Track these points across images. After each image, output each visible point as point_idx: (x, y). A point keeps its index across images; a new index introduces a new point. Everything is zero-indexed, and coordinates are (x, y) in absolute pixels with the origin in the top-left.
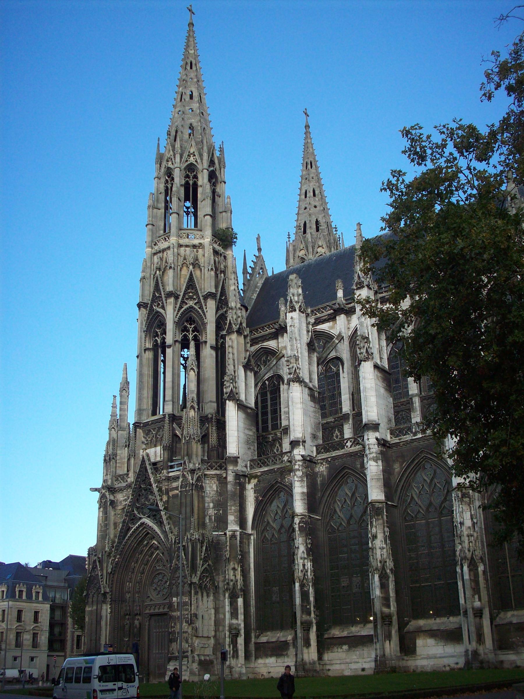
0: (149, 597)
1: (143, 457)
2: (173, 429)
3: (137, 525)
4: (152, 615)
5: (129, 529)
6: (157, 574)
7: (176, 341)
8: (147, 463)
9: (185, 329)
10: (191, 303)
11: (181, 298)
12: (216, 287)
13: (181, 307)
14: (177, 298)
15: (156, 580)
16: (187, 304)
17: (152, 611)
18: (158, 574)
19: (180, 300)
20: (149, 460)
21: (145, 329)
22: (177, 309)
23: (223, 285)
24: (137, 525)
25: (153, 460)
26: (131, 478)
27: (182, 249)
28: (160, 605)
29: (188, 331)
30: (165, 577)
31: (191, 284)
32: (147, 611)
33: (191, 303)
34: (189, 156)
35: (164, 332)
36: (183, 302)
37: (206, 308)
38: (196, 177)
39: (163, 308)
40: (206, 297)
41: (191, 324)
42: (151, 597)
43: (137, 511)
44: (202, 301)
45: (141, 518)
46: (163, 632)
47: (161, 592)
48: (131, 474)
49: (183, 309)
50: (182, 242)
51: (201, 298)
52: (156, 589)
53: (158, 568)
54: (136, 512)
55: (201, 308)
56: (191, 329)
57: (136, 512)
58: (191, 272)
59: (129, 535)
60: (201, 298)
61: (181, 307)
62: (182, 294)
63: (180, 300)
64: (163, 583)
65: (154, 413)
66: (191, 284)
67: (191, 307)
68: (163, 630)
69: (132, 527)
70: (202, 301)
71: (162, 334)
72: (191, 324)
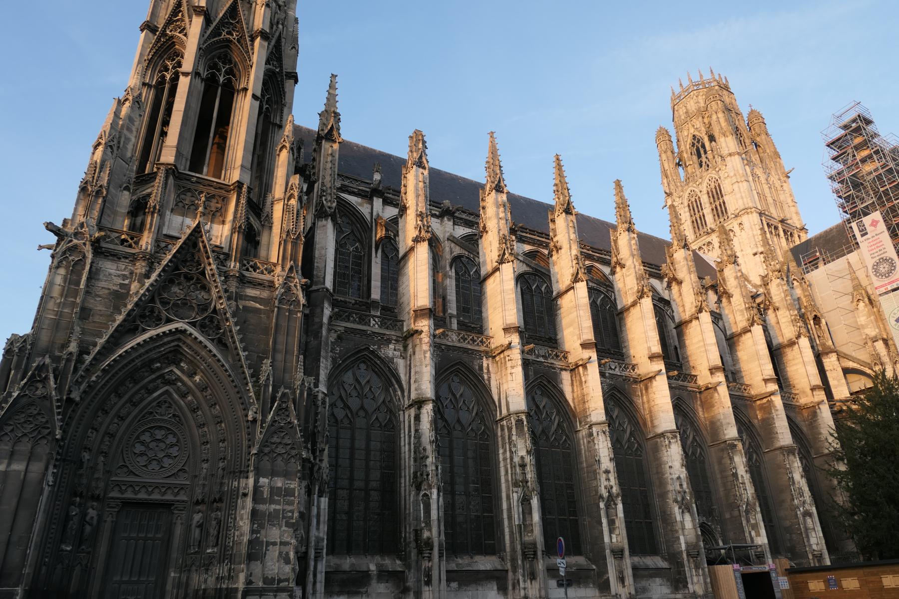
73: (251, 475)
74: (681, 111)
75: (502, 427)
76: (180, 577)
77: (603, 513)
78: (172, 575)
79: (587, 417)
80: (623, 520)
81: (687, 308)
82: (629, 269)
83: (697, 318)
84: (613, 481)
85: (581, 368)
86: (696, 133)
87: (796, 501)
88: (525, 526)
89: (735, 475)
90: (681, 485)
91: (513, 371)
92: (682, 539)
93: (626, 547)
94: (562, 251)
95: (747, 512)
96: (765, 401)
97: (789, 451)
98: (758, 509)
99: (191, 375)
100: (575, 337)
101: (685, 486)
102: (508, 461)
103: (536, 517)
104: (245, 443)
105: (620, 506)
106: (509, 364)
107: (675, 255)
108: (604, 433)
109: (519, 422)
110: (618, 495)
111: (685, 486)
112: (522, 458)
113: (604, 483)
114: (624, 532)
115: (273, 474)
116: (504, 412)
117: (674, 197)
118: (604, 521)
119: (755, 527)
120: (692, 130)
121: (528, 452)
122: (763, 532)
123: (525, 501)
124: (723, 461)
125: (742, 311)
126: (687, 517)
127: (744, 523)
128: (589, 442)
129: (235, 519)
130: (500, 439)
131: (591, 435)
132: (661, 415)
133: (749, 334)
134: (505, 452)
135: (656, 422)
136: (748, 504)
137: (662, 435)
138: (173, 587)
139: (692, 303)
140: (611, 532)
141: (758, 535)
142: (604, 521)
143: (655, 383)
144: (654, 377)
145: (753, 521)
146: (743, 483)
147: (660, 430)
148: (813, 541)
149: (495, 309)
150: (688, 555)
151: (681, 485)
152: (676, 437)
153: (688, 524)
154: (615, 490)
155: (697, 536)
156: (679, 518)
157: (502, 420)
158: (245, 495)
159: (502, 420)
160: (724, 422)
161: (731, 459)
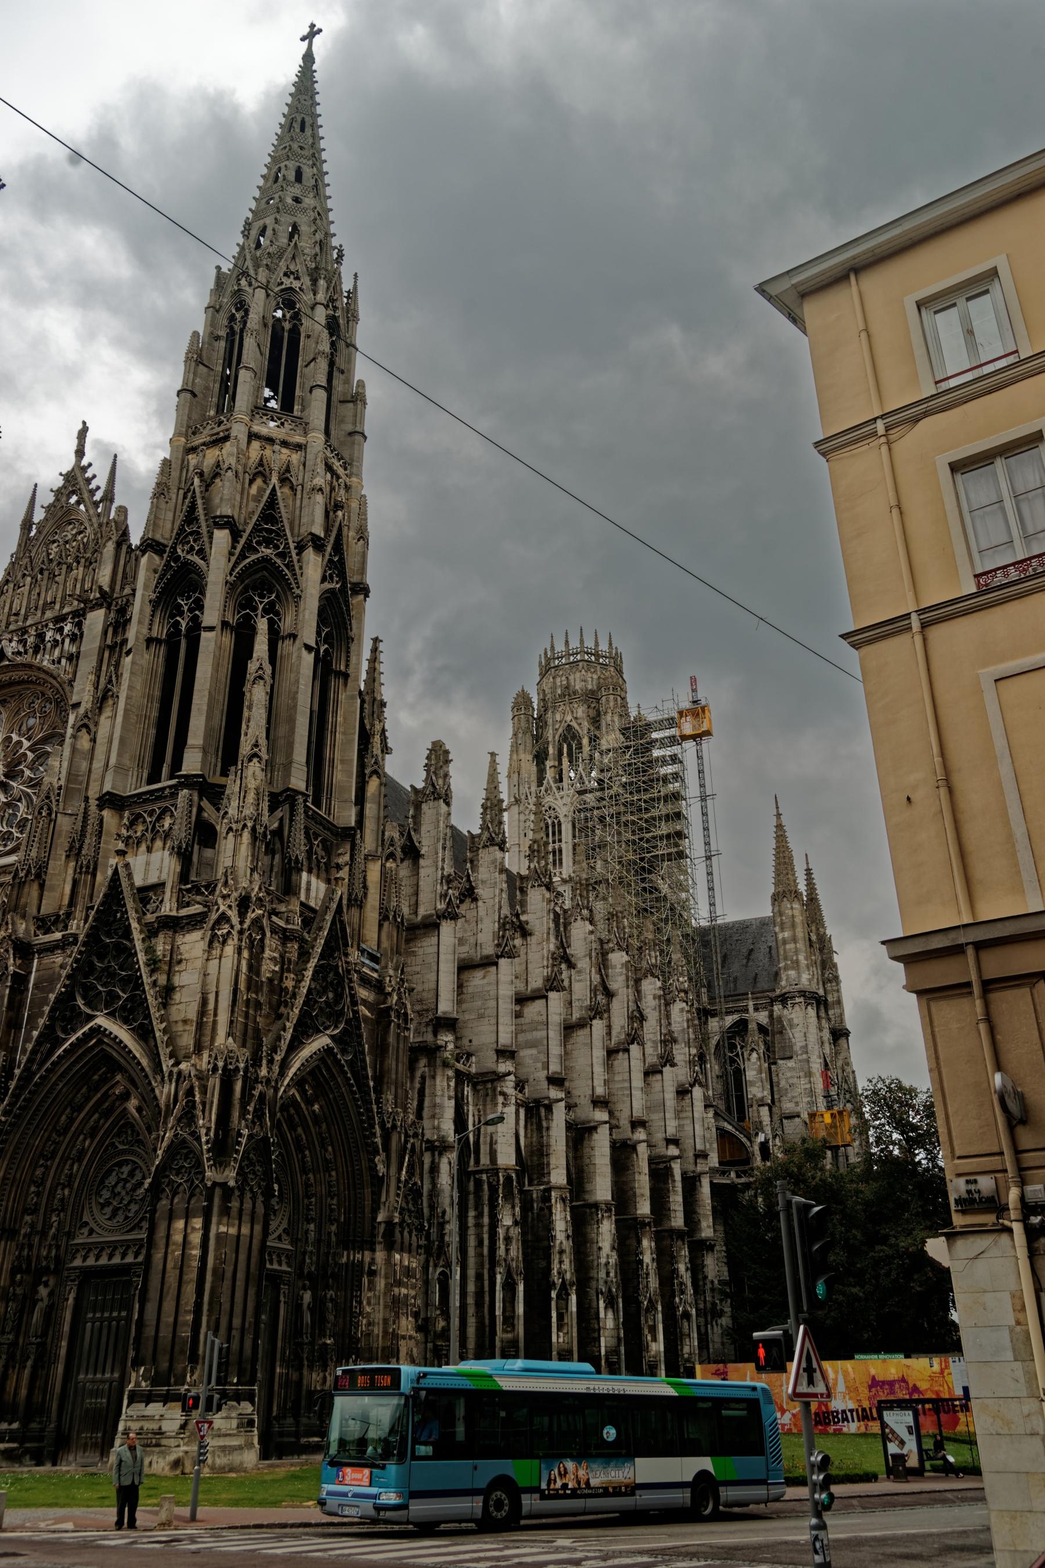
0: (87, 1224)
1: (116, 872)
2: (200, 810)
3: (79, 1034)
4: (87, 1275)
5: (58, 1042)
6: (116, 1165)
7: (225, 624)
8: (124, 883)
9: (248, 604)
10: (266, 551)
11: (245, 536)
12: (327, 530)
13: (242, 556)
14: (236, 535)
15: (112, 1180)
16: (257, 551)
17: (91, 1261)
18: (120, 1164)
19: (242, 541)
20: (130, 876)
21: (153, 596)
22: (233, 559)
23: (340, 529)
24: (79, 1034)
25: (138, 882)
26: (78, 926)
27: (256, 444)
28: (114, 1246)
29: (255, 609)
30: (137, 1172)
31: (270, 511)
32: (78, 1262)
33: (266, 551)
34: (286, 274)
35: (199, 605)
36: (249, 548)
37: (301, 568)
38: (296, 316)
39: (202, 553)
40: (301, 548)
41: (262, 596)
42: (92, 1225)
43: (84, 998)
44: (294, 553)
45: (91, 1018)
46: (114, 1319)
47: (120, 1212)
48: (79, 913)
49: (248, 561)
50: (256, 428)
51: (292, 546)
52: (108, 1203)
53: (121, 1147)
54: (80, 1002)
55: (290, 566)
56: (261, 607)
57: (80, 1002)
58: (274, 489)
59: (54, 1058)
60: (292, 546)
61: (242, 556)
62: (248, 532)
63: (242, 541)
64: (129, 1186)
65: (154, 778)
66: (270, 511)
67: (265, 560)
68: (115, 1314)
69: (65, 1040)
70: (294, 553)
71: (190, 610)
72: (262, 596)
73: (378, 1247)
74: (558, 680)
75: (479, 1184)
76: (287, 1374)
77: (553, 1304)
78: (278, 1370)
79: (543, 1175)
80: (575, 1316)
81: (614, 1033)
82: (579, 972)
83: (627, 1051)
84: (566, 1266)
85: (543, 1111)
86: (574, 724)
87: (677, 1300)
88: (509, 1320)
89: (641, 1262)
90: (608, 1274)
91: (506, 1110)
92: (602, 1340)
93: (575, 1349)
94: (533, 940)
95: (647, 1310)
96: (662, 1166)
97: (679, 1234)
98: (660, 1308)
99: (309, 1102)
100: (539, 1065)
101: (612, 1274)
102: (486, 1229)
103: (520, 1309)
104: (368, 1202)
105: (574, 1298)
106: (500, 1099)
107: (611, 956)
108: (563, 1200)
109: (508, 1179)
110: (572, 1284)
111: (612, 1274)
112: (508, 1228)
113: (555, 1266)
114: (575, 1330)
115: (401, 1250)
116: (485, 1160)
117: (522, 808)
118: (554, 1314)
119: (653, 1329)
120: (569, 718)
121: (516, 1223)
122: (661, 1337)
123: (510, 1287)
124: (628, 1242)
125: (654, 1042)
126: (610, 1315)
127: (643, 1321)
128: (542, 1209)
129: (360, 1303)
130: (471, 1197)
131: (546, 1198)
132: (598, 1179)
133: (658, 1077)
134: (480, 1215)
135: (588, 1187)
136: (650, 1300)
137: (596, 1206)
138: (280, 1385)
139: (623, 1027)
140: (559, 1329)
141: (655, 1339)
142: (554, 1314)
143: (595, 1136)
144: (595, 1128)
145: (651, 1323)
146: (648, 1274)
147: (591, 1199)
148: (686, 1349)
149: (481, 1016)
150: (607, 1359)
151: (608, 1274)
152: (610, 1210)
153: (610, 1323)
154: (568, 1276)
155: (619, 1339)
156: (602, 1315)
157: (481, 1172)
158: (372, 1273)
159: (481, 1172)
160: (638, 1192)
161: (639, 1242)
